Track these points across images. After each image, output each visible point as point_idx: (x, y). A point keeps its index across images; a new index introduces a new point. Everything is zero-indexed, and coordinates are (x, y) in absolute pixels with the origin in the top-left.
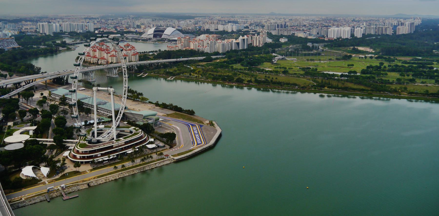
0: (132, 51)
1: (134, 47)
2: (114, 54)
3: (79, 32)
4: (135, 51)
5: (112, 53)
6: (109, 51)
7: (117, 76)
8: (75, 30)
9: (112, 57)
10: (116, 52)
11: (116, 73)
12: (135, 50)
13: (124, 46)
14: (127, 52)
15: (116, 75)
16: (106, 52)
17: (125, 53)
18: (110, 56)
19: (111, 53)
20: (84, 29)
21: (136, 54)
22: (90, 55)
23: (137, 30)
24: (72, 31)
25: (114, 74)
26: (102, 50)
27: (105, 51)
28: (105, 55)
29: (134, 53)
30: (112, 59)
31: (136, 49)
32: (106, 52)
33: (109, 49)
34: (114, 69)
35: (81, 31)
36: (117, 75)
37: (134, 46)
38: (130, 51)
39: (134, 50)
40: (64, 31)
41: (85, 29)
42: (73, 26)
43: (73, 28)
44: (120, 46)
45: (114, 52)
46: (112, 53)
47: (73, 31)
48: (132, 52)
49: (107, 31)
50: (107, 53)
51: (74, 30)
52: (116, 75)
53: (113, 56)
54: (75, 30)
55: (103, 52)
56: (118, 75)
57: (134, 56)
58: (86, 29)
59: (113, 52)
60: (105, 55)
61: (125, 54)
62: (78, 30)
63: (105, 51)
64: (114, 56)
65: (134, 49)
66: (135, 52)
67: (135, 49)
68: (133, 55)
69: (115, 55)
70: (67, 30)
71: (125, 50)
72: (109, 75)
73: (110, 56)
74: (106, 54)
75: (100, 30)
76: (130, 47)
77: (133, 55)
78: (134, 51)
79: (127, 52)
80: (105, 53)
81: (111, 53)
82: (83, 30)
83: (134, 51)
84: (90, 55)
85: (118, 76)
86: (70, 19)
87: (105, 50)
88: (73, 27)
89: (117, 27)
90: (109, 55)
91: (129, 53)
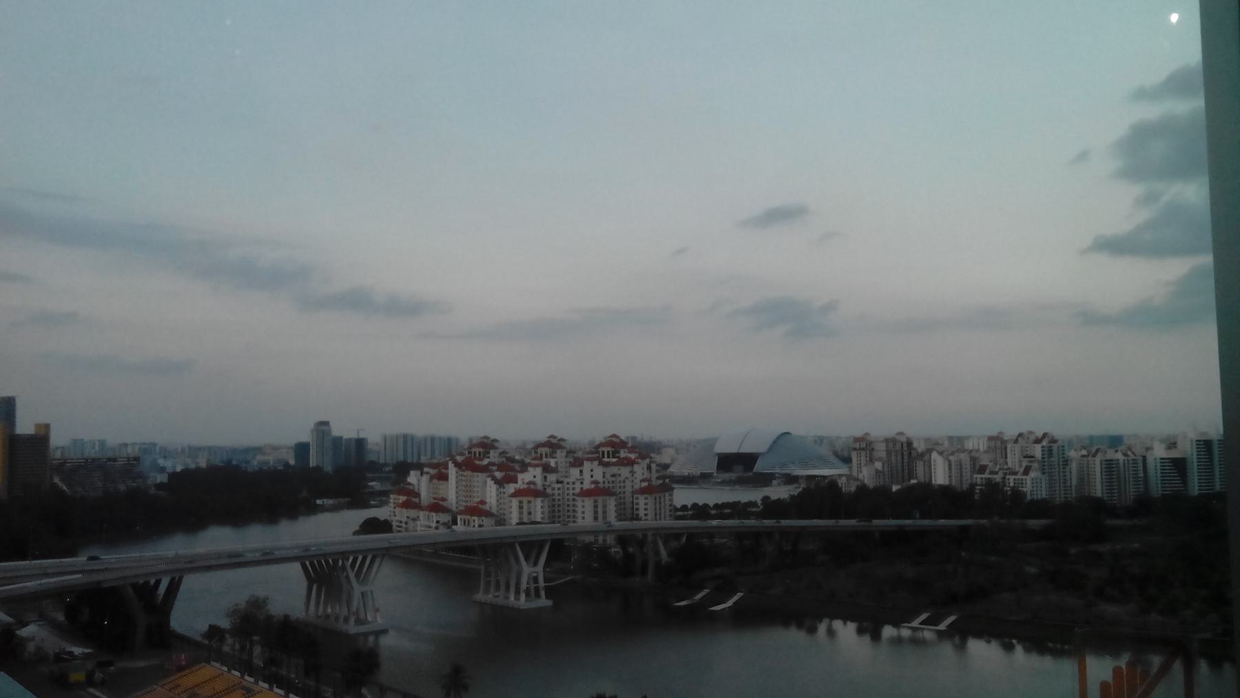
2: (539, 480)
7: (544, 602)
9: (525, 500)
10: (547, 469)
15: (538, 595)
18: (514, 495)
22: (416, 500)
25: (524, 586)
28: (490, 494)
32: (494, 478)
34: (527, 559)
36: (543, 593)
45: (539, 471)
50: (500, 483)
53: (531, 492)
55: (480, 477)
56: (547, 597)
57: (650, 500)
60: (490, 494)
61: (596, 482)
63: (492, 471)
64: (536, 493)
68: (643, 491)
69: (540, 487)
71: (596, 463)
72: (490, 598)
73: (514, 495)
74: (494, 487)
77: (643, 491)
80: (490, 482)
84: (416, 500)
85: (549, 603)
90: (511, 488)
91: (619, 479)
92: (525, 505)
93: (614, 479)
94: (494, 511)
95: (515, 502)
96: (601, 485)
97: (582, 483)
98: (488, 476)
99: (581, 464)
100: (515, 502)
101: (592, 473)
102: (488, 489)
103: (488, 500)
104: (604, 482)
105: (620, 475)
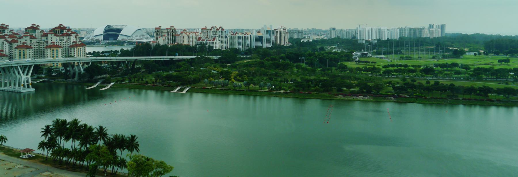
2: (28, 43)
5: (23, 40)
9: (22, 50)
11: (28, 81)
14: (58, 40)
15: (28, 86)
16: (10, 40)
17: (55, 42)
18: (16, 48)
19: (19, 40)
30: (22, 54)
32: (7, 41)
34: (23, 73)
38: (68, 37)
46: (23, 40)
48: (72, 41)
50: (10, 43)
52: (28, 86)
59: (24, 37)
61: (53, 43)
63: (6, 38)
71: (54, 35)
74: (7, 45)
79: (58, 40)
80: (5, 42)
81: (19, 40)
90: (15, 45)
91: (63, 41)
92: (22, 52)
93: (61, 41)
94: (8, 54)
95: (17, 51)
96: (55, 44)
97: (47, 43)
98: (4, 40)
99: (47, 36)
101: (51, 39)
102: (4, 45)
103: (4, 50)
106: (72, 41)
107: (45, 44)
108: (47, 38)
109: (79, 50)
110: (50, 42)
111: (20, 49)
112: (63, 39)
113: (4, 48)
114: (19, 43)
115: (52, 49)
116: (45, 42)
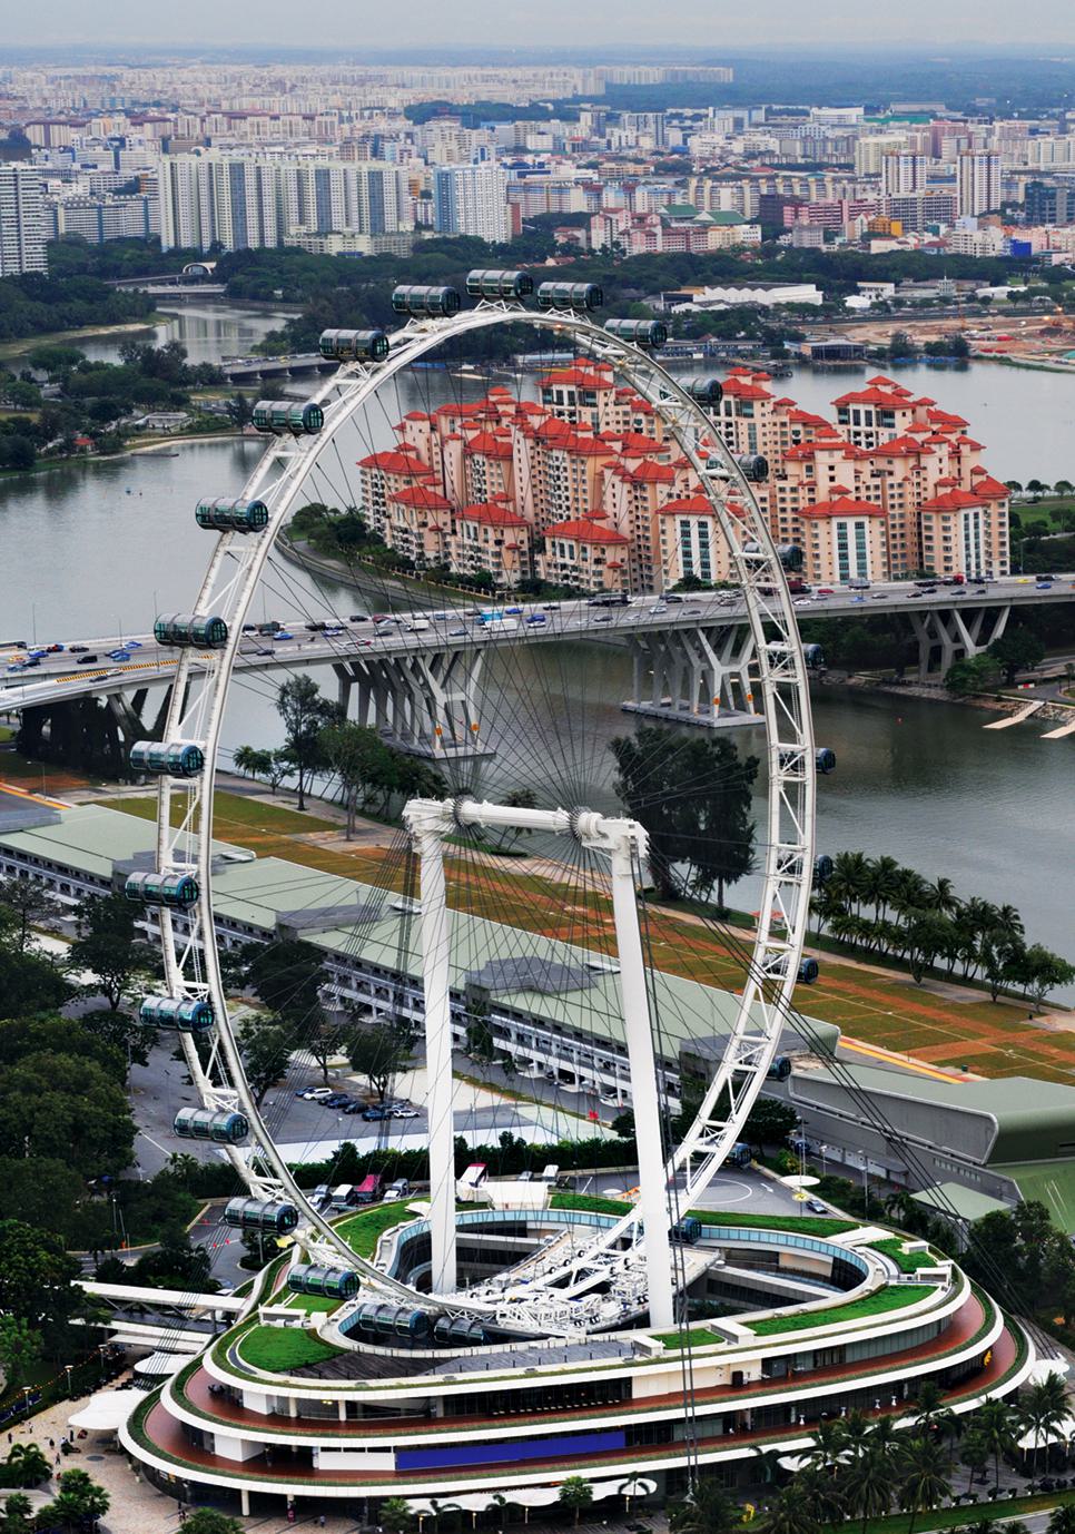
0: (927, 461)
1: (956, 423)
3: (335, 246)
4: (971, 460)
6: (653, 458)
8: (295, 233)
12: (965, 449)
13: (843, 411)
14: (866, 476)
16: (632, 465)
17: (850, 485)
18: (669, 511)
20: (390, 222)
21: (974, 491)
23: (1021, 236)
24: (253, 244)
26: (578, 451)
27: (605, 460)
29: (956, 481)
31: (976, 447)
32: (618, 469)
33: (658, 436)
35: (364, 246)
37: (951, 412)
38: (912, 462)
39: (956, 455)
40: (168, 242)
41: (408, 226)
42: (268, 190)
43: (269, 211)
44: (792, 404)
47: (271, 243)
48: (933, 476)
49: (660, 246)
50: (636, 482)
51: (281, 229)
54: (293, 230)
55: (593, 465)
58: (419, 227)
61: (843, 491)
62: (325, 231)
63: (611, 452)
65: (953, 438)
66: (966, 473)
67: (963, 441)
70: (206, 232)
71: (843, 453)
73: (669, 511)
75: (580, 234)
76: (902, 423)
78: (949, 468)
79: (866, 476)
80: (608, 473)
81: (679, 475)
82: (377, 228)
83: (949, 468)
86: (242, 116)
87: (617, 446)
88: (269, 200)
89: (788, 211)
90: (659, 494)
91: (890, 480)
92: (694, 531)
93: (877, 481)
96: (852, 497)
97: (811, 490)
98: (606, 466)
99: (810, 457)
100: (673, 527)
101: (832, 473)
102: (609, 491)
104: (857, 489)
105: (891, 473)
106: (933, 476)
107: (803, 493)
108: (809, 469)
109: (972, 521)
110: (824, 486)
111: (684, 518)
112: (889, 468)
113: (608, 498)
114: (678, 487)
115: (835, 521)
116: (801, 484)
